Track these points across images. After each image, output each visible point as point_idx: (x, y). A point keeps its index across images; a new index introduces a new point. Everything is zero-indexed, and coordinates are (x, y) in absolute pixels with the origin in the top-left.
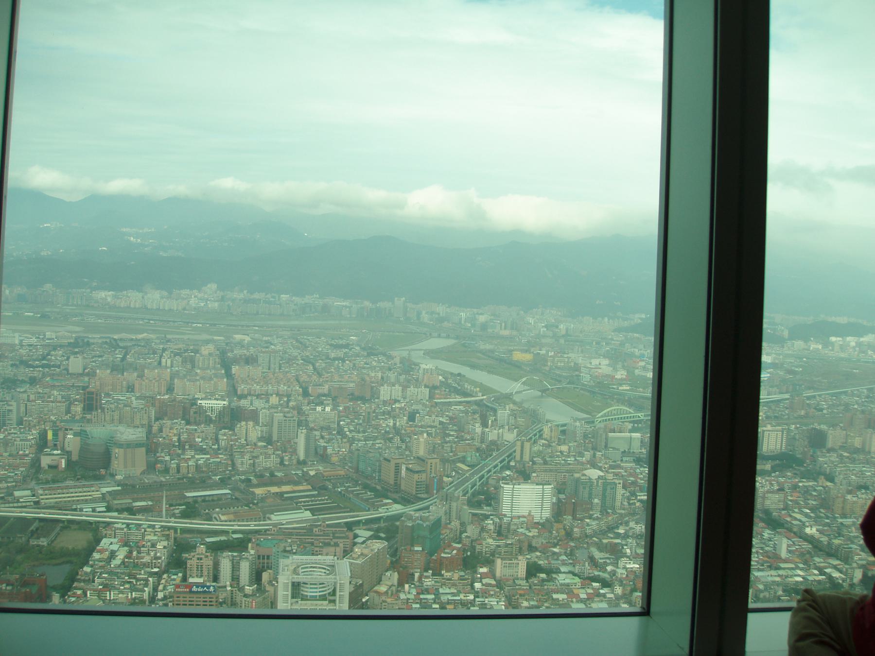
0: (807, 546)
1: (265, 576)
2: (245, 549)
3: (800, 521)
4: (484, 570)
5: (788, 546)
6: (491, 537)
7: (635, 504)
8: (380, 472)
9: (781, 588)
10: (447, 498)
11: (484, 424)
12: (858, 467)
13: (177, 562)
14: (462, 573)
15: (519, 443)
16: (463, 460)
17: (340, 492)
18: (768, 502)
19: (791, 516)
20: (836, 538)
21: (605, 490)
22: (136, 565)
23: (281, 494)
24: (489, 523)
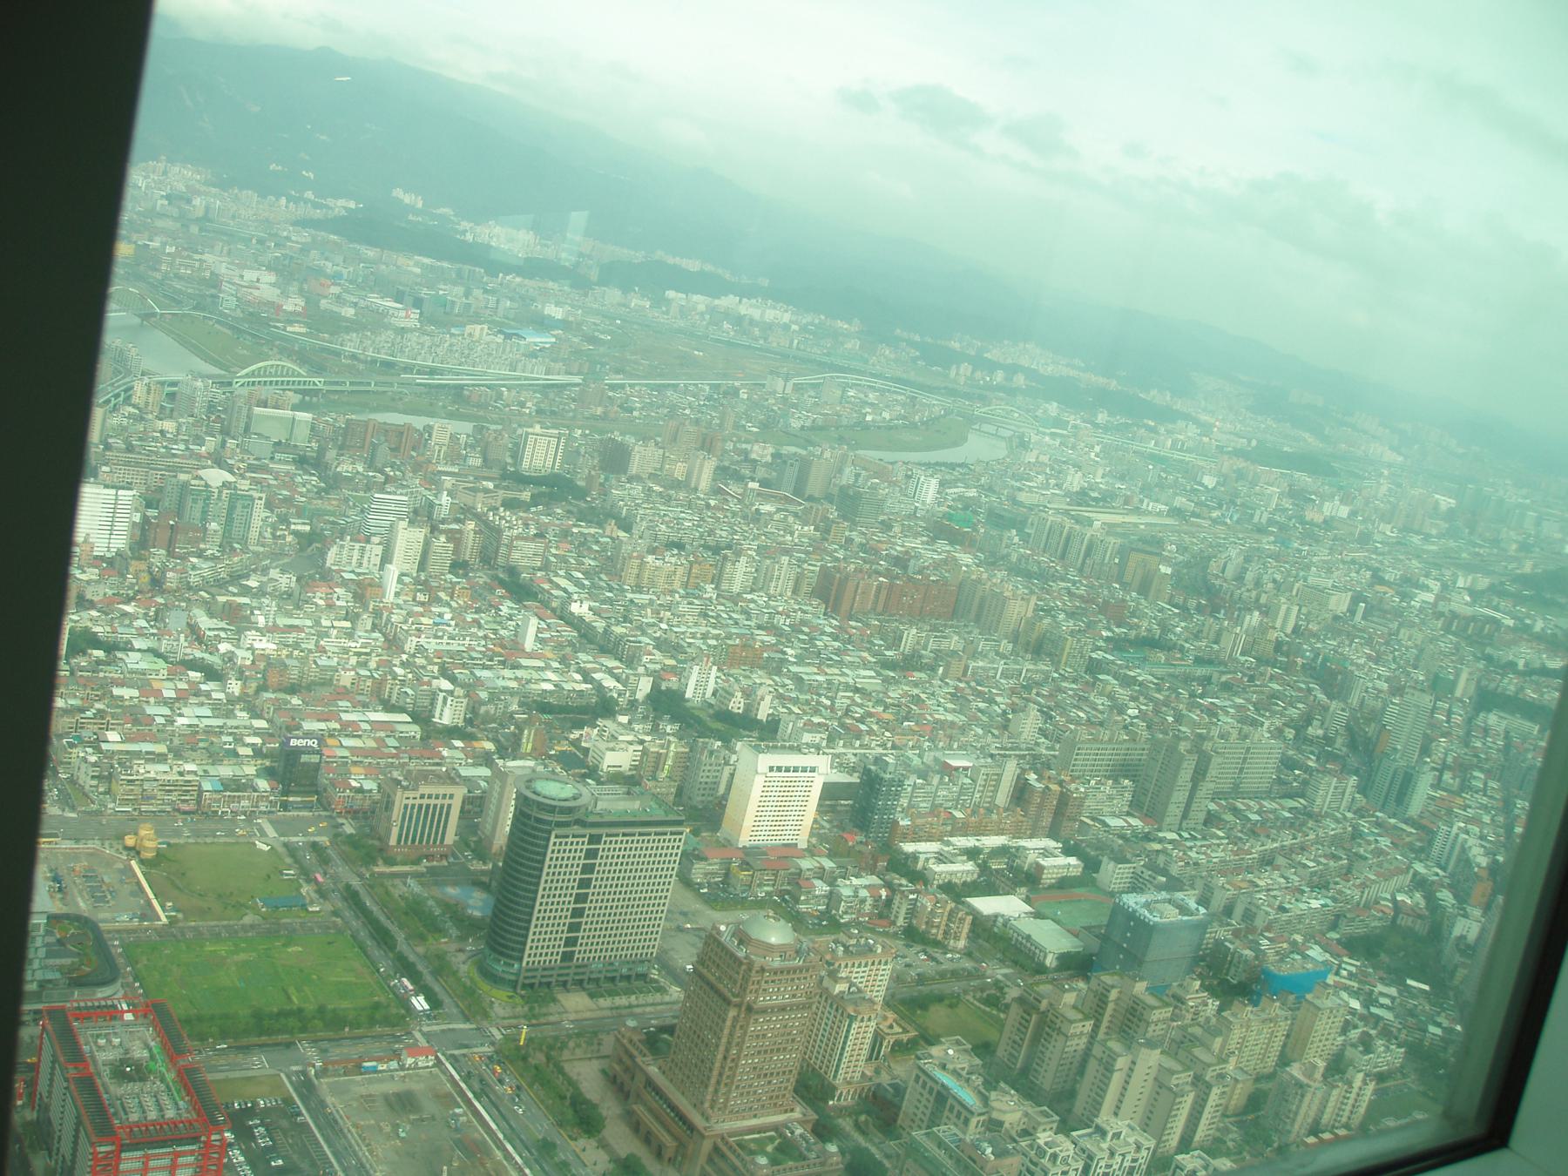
0: (569, 633)
3: (565, 590)
5: (539, 630)
7: (284, 537)
9: (516, 700)
12: (674, 511)
18: (516, 555)
19: (551, 581)
21: (231, 508)
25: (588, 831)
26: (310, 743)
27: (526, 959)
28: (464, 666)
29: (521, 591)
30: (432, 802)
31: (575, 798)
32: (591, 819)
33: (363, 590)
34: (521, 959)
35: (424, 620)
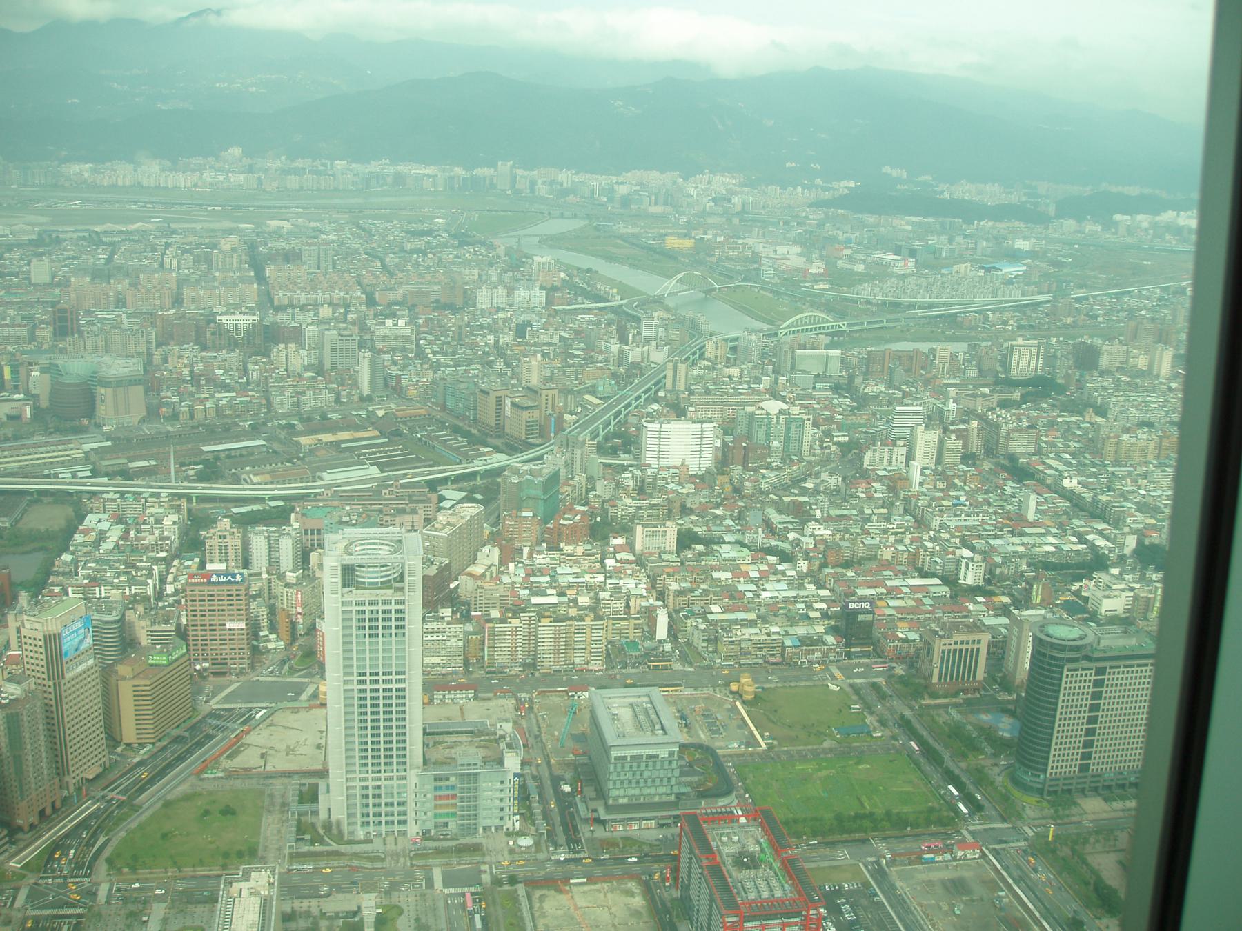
0: (1063, 504)
1: (314, 557)
2: (287, 521)
4: (619, 541)
5: (1038, 504)
6: (629, 496)
7: (829, 447)
8: (475, 409)
9: (1025, 561)
10: (569, 444)
11: (623, 340)
12: (1140, 396)
13: (192, 543)
14: (589, 547)
15: (670, 366)
16: (593, 391)
17: (420, 439)
18: (1013, 445)
19: (1044, 463)
20: (1103, 493)
21: (788, 429)
22: (134, 550)
23: (336, 445)
24: (627, 478)
25: (1094, 665)
26: (864, 605)
27: (1049, 771)
28: (980, 537)
29: (1021, 474)
30: (964, 647)
31: (1081, 638)
32: (1096, 654)
33: (895, 483)
34: (1045, 771)
35: (945, 503)
